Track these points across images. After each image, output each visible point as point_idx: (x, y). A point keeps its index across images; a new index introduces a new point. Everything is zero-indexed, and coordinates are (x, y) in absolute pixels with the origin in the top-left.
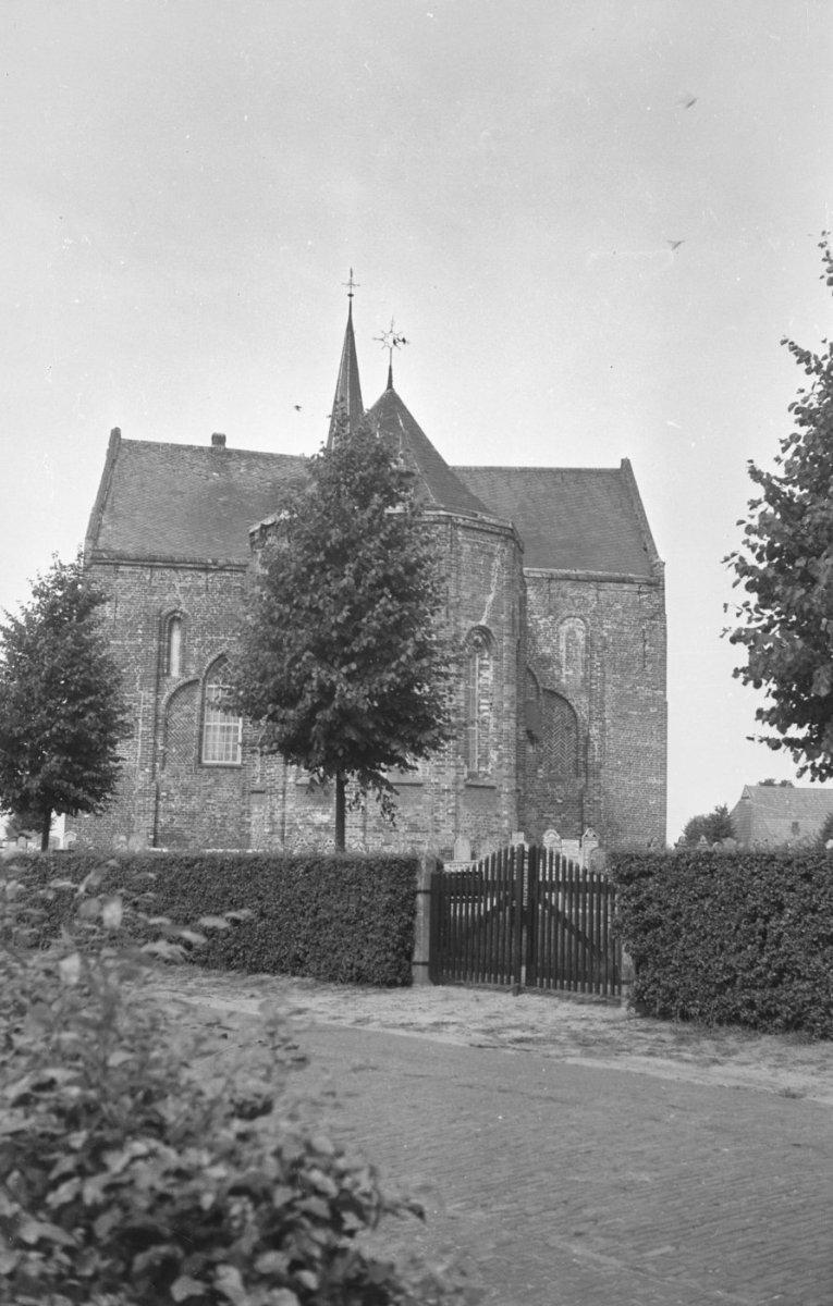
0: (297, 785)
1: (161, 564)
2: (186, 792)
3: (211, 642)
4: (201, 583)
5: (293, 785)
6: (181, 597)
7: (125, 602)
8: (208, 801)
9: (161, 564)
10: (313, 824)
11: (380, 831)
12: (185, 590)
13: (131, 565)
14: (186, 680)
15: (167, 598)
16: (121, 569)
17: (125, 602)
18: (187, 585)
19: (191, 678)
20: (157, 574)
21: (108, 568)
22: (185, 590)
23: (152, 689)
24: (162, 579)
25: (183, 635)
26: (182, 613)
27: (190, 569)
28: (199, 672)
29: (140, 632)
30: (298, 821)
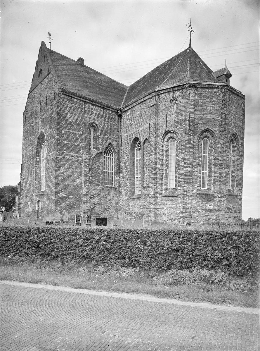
0: (198, 194)
1: (88, 101)
2: (99, 196)
3: (106, 138)
4: (102, 113)
5: (196, 194)
6: (95, 117)
7: (76, 115)
8: (106, 200)
9: (88, 101)
10: (205, 209)
11: (228, 212)
12: (97, 115)
13: (77, 99)
14: (98, 152)
15: (91, 116)
16: (73, 99)
17: (76, 115)
18: (97, 113)
19: (100, 151)
20: (87, 105)
21: (68, 97)
22: (97, 115)
23: (88, 154)
24: (88, 108)
25: (95, 131)
26: (96, 124)
27: (98, 106)
28: (102, 149)
29: (81, 129)
30: (198, 208)
